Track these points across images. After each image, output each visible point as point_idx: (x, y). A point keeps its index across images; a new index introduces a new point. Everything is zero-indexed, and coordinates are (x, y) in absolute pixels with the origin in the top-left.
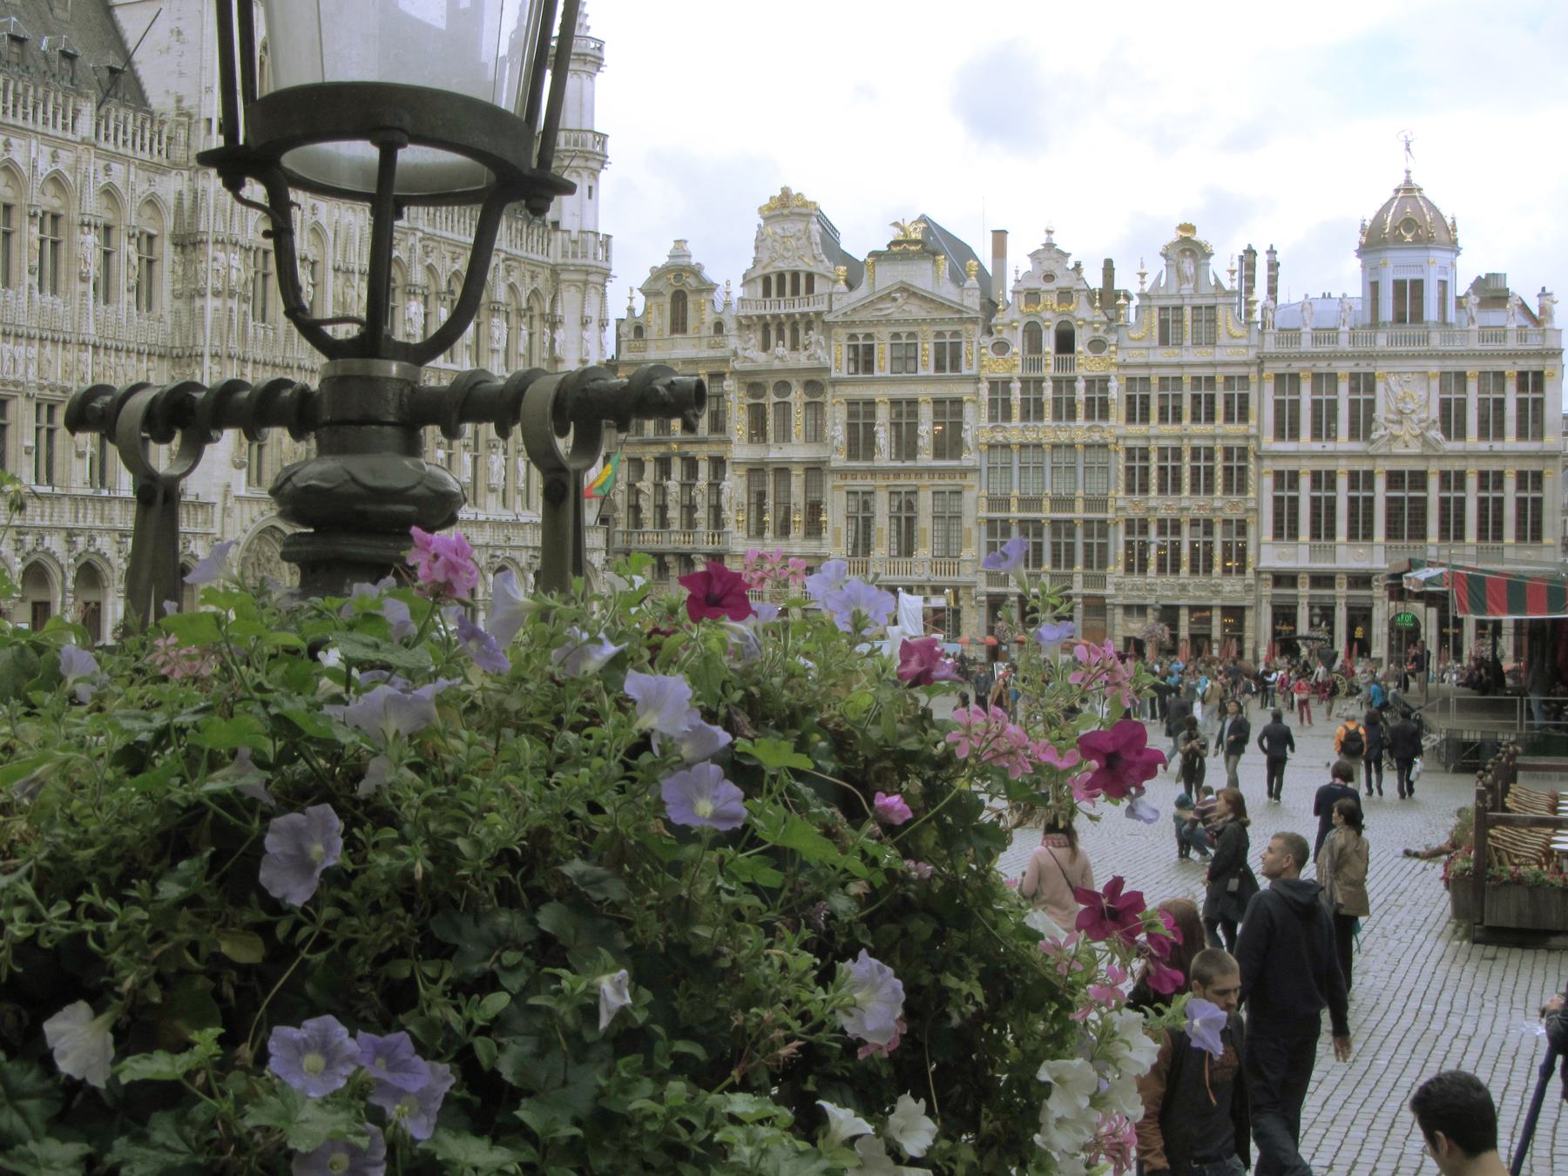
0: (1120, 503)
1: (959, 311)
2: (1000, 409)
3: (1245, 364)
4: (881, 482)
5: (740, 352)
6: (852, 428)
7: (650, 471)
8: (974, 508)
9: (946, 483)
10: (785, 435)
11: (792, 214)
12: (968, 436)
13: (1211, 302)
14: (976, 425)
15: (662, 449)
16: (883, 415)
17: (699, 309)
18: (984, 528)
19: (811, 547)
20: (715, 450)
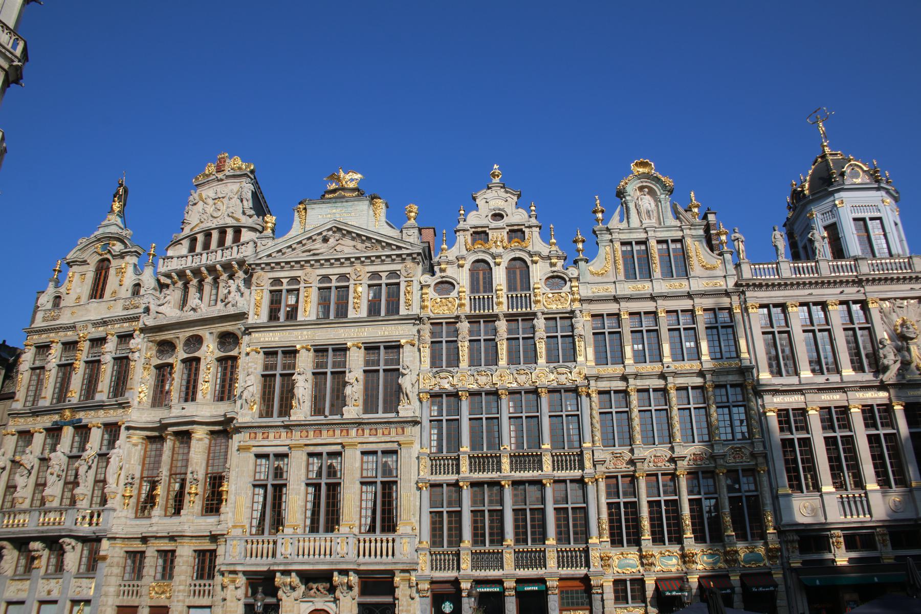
0: (599, 456)
1: (399, 248)
2: (444, 355)
3: (727, 294)
4: (297, 437)
5: (153, 308)
6: (267, 379)
7: (39, 439)
8: (413, 470)
9: (378, 440)
10: (190, 394)
11: (228, 177)
12: (406, 382)
13: (678, 234)
14: (417, 370)
15: (56, 418)
16: (305, 362)
17: (121, 271)
18: (426, 493)
19: (209, 524)
20: (112, 416)
